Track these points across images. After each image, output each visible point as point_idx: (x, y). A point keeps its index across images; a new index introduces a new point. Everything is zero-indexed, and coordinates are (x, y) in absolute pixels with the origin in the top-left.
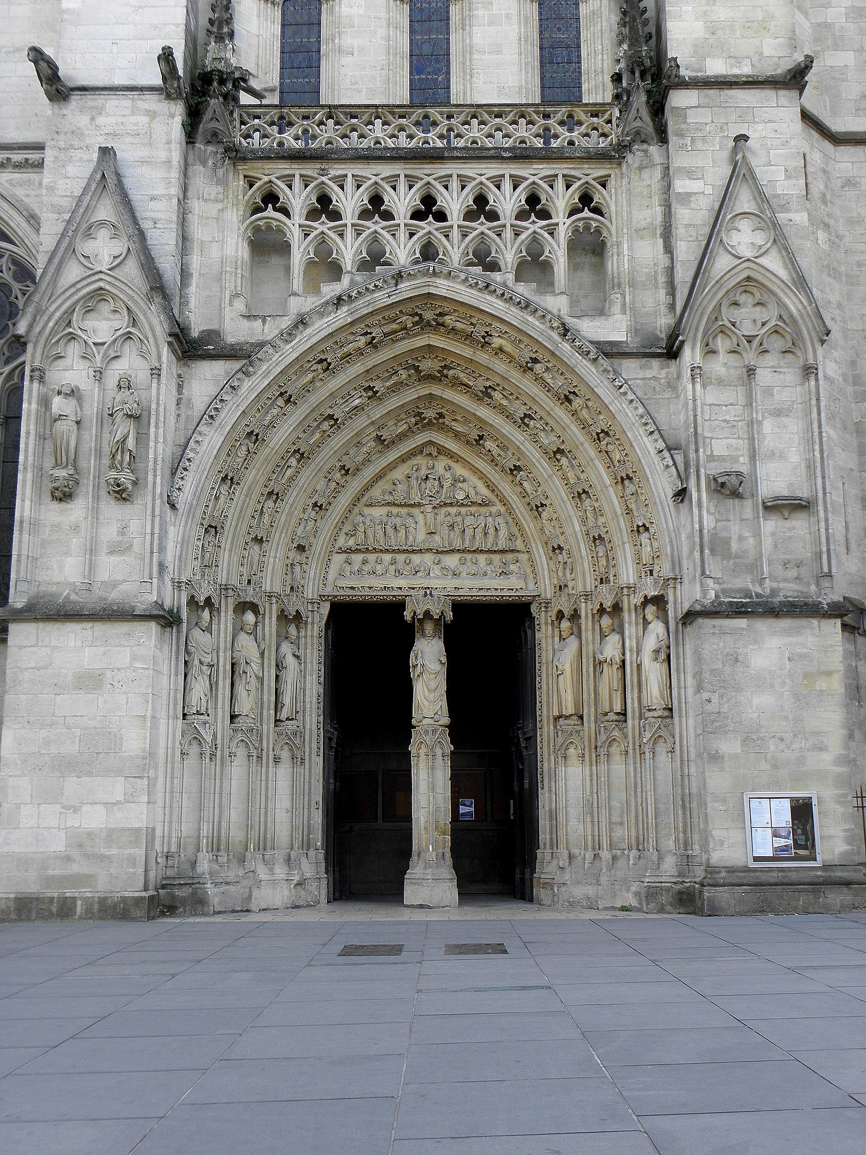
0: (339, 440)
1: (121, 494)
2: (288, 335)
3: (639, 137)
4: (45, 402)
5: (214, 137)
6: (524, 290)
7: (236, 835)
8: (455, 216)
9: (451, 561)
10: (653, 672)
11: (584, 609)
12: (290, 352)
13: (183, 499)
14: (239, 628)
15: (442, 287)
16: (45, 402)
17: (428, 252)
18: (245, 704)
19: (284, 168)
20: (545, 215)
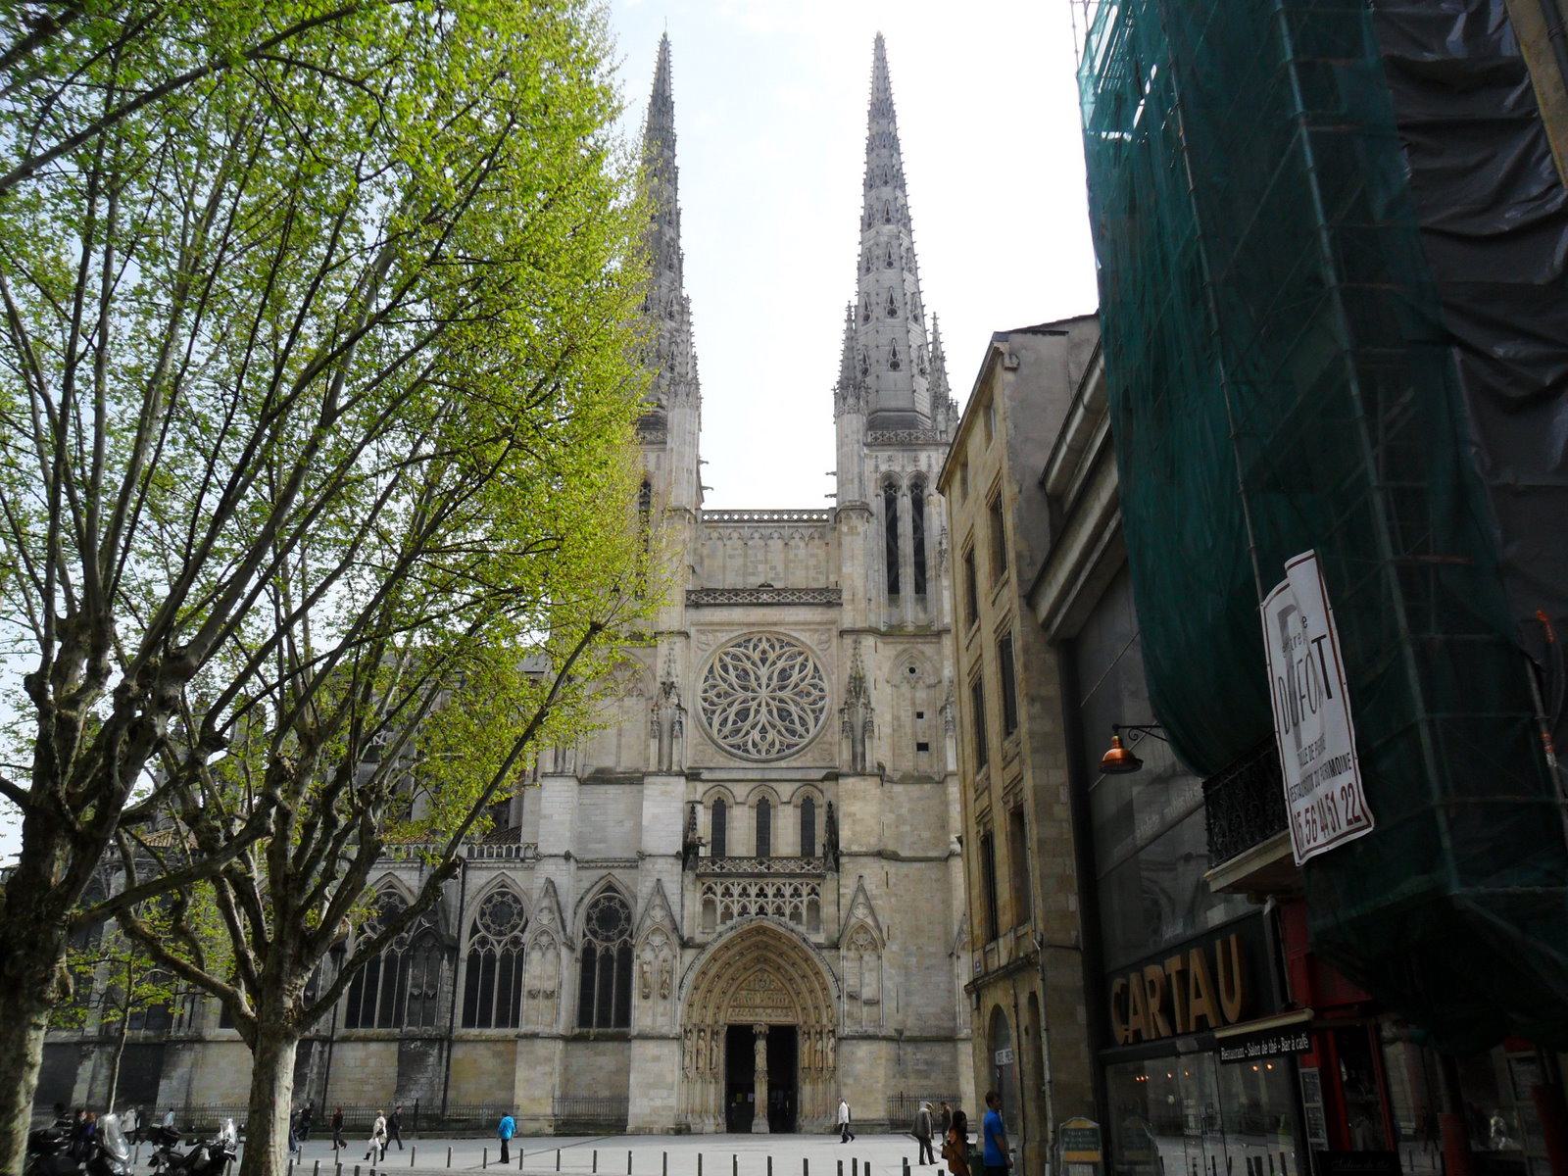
0: (731, 970)
1: (664, 997)
2: (715, 940)
3: (830, 869)
4: (641, 966)
5: (692, 869)
6: (792, 924)
7: (698, 1107)
8: (770, 895)
9: (769, 1011)
10: (831, 1055)
11: (812, 1031)
12: (717, 945)
13: (682, 997)
14: (699, 1037)
15: (766, 923)
16: (641, 966)
17: (761, 910)
18: (701, 1065)
19: (714, 879)
20: (800, 896)
